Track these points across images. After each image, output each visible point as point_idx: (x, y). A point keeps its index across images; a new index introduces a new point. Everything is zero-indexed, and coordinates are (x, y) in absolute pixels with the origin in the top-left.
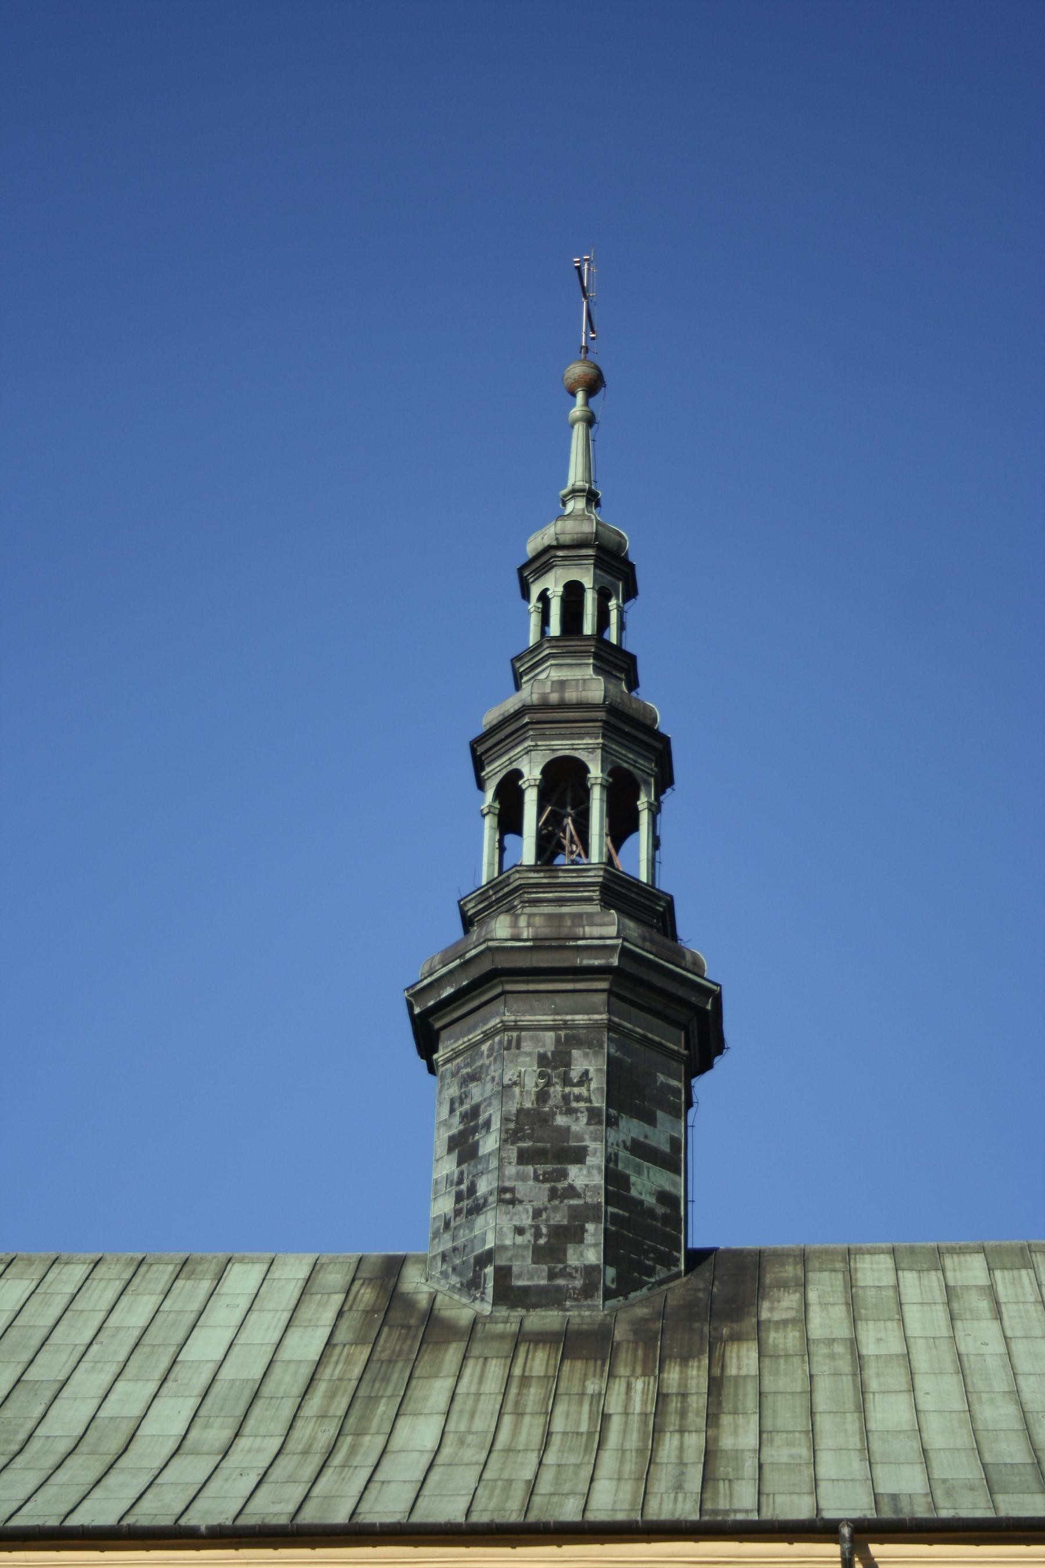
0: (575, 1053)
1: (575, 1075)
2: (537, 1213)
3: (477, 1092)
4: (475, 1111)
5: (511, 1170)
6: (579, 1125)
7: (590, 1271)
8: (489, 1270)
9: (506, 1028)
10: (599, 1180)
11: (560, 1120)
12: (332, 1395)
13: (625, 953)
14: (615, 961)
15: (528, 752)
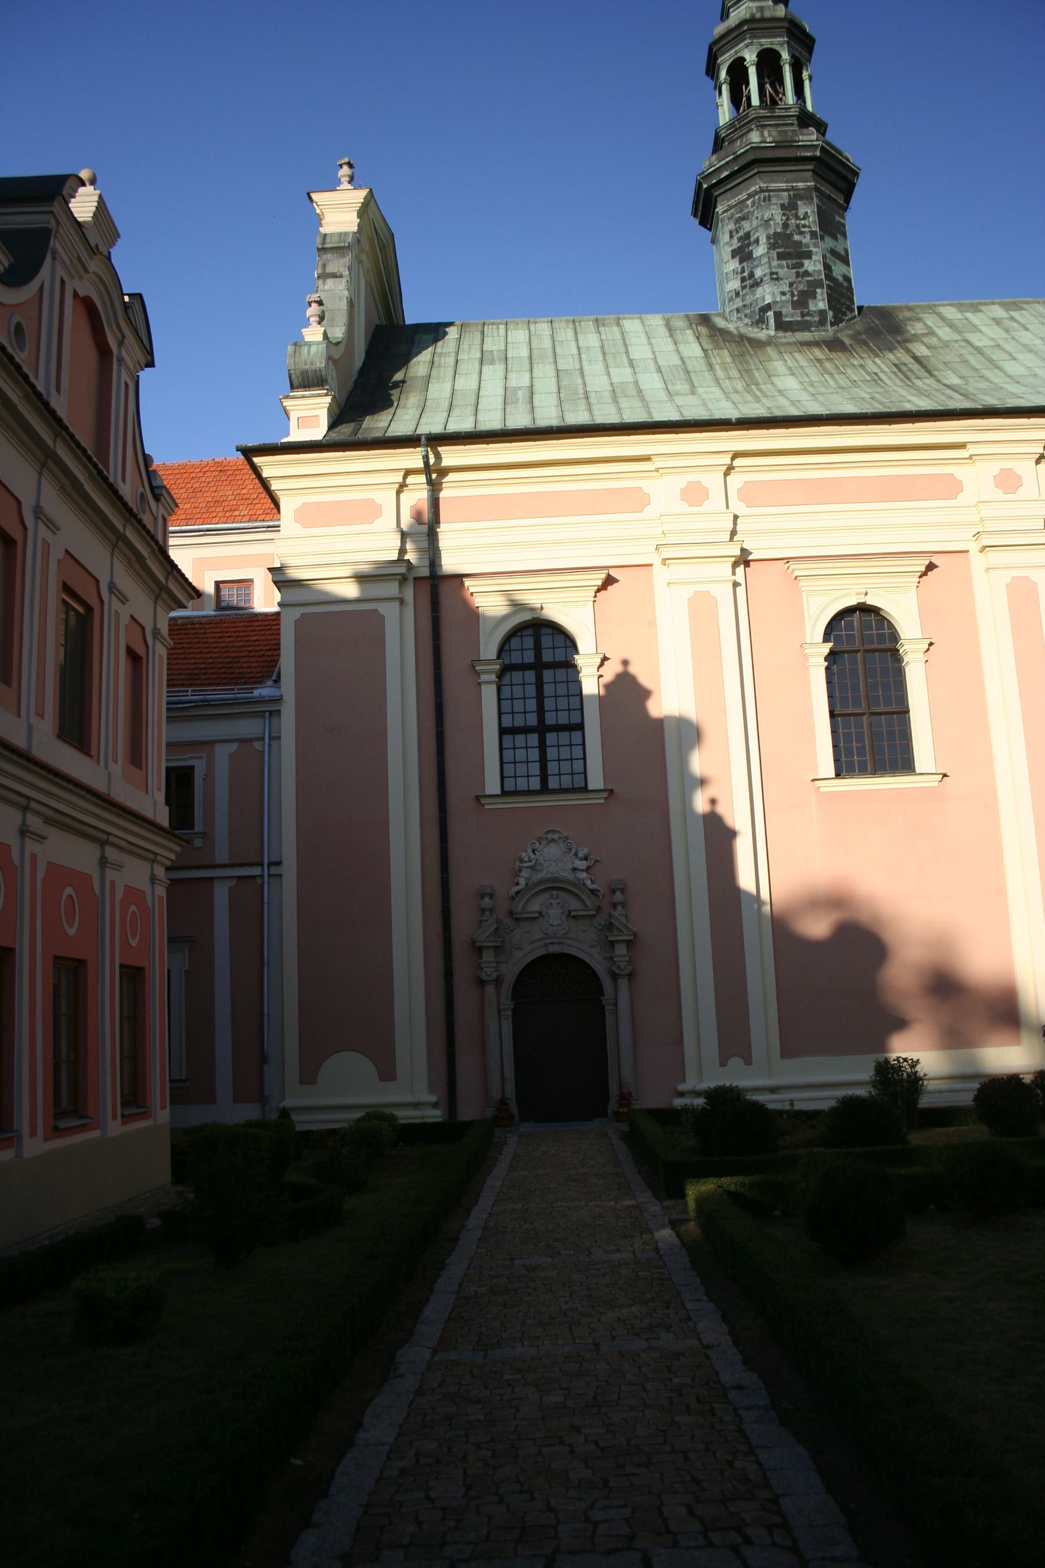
1: (801, 212)
2: (791, 285)
3: (746, 226)
4: (748, 235)
5: (775, 263)
6: (807, 239)
7: (822, 313)
8: (770, 314)
9: (762, 191)
10: (820, 267)
11: (796, 238)
13: (823, 149)
14: (818, 154)
15: (747, 46)
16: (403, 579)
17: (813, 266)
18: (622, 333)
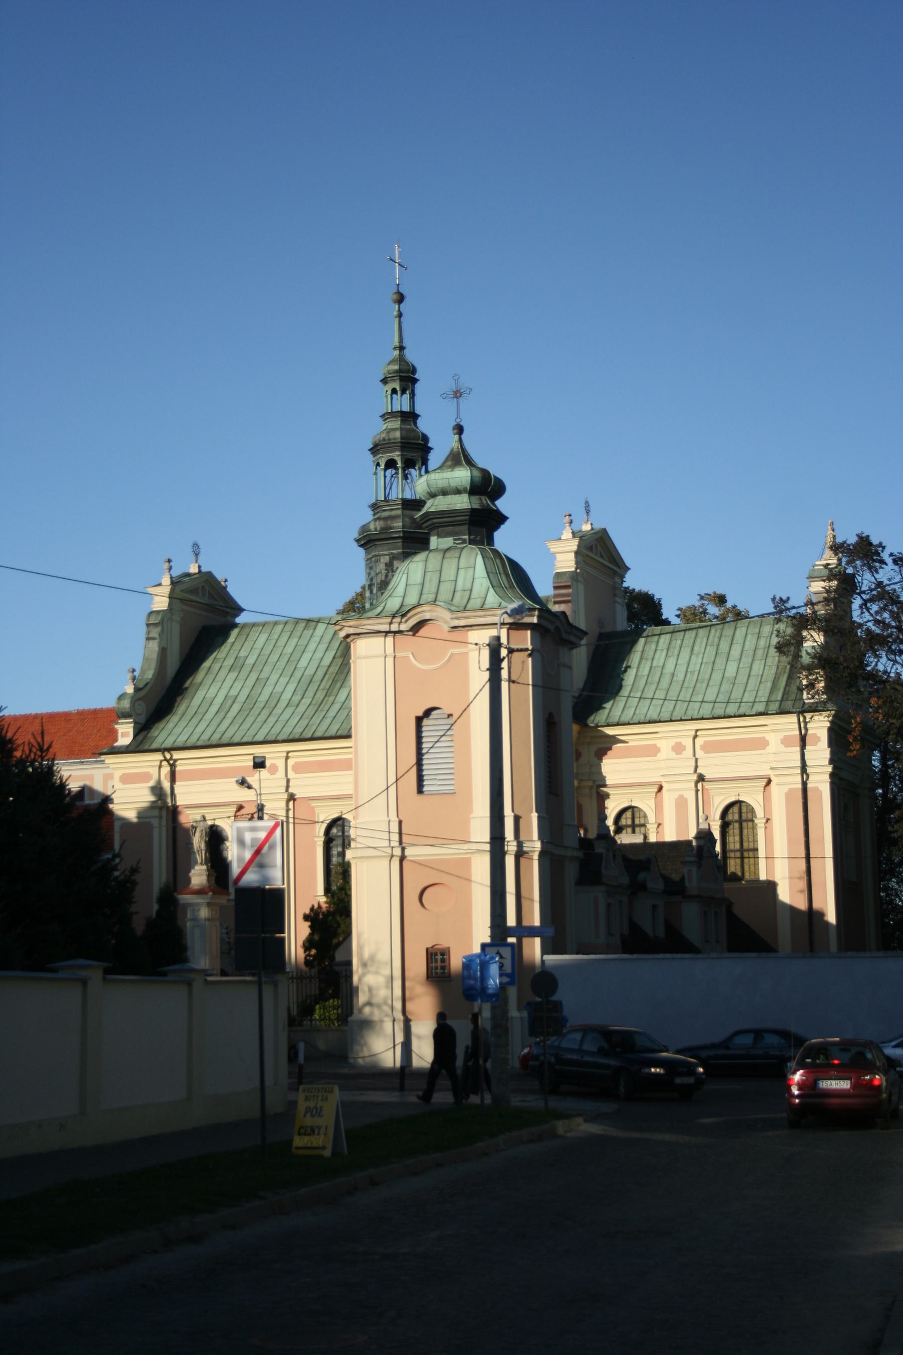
0: (395, 562)
9: (376, 556)
12: (328, 681)
13: (404, 532)
14: (401, 535)
16: (161, 808)
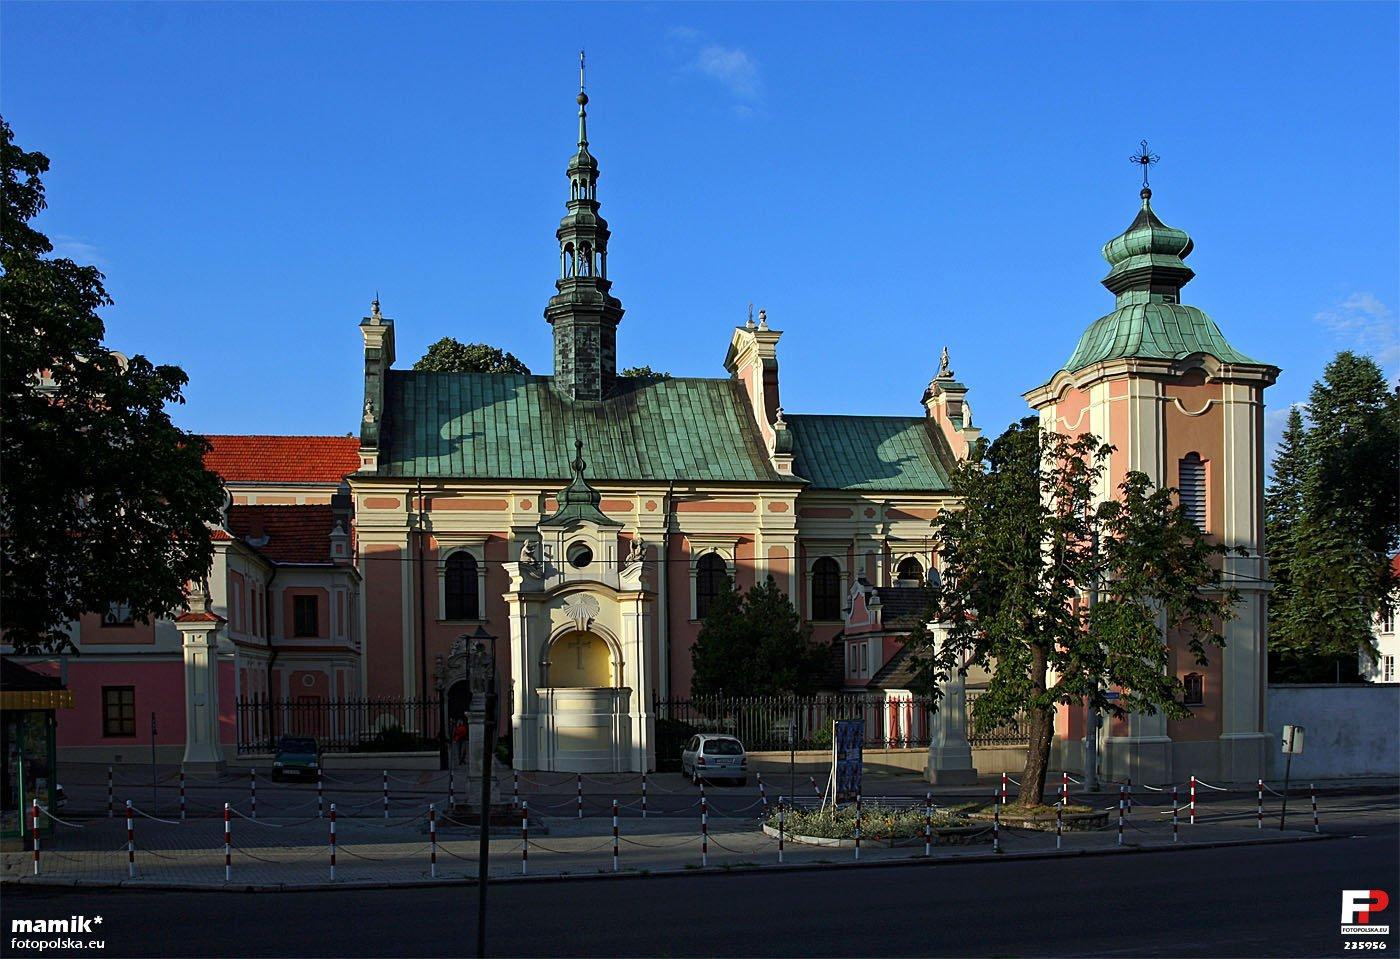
1: (593, 337)
2: (584, 375)
4: (566, 345)
11: (589, 351)
12: (547, 430)
17: (596, 366)
18: (505, 390)
